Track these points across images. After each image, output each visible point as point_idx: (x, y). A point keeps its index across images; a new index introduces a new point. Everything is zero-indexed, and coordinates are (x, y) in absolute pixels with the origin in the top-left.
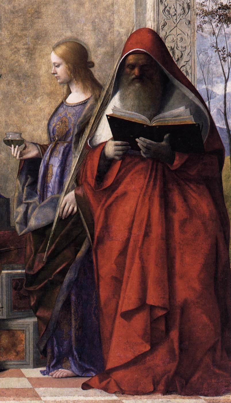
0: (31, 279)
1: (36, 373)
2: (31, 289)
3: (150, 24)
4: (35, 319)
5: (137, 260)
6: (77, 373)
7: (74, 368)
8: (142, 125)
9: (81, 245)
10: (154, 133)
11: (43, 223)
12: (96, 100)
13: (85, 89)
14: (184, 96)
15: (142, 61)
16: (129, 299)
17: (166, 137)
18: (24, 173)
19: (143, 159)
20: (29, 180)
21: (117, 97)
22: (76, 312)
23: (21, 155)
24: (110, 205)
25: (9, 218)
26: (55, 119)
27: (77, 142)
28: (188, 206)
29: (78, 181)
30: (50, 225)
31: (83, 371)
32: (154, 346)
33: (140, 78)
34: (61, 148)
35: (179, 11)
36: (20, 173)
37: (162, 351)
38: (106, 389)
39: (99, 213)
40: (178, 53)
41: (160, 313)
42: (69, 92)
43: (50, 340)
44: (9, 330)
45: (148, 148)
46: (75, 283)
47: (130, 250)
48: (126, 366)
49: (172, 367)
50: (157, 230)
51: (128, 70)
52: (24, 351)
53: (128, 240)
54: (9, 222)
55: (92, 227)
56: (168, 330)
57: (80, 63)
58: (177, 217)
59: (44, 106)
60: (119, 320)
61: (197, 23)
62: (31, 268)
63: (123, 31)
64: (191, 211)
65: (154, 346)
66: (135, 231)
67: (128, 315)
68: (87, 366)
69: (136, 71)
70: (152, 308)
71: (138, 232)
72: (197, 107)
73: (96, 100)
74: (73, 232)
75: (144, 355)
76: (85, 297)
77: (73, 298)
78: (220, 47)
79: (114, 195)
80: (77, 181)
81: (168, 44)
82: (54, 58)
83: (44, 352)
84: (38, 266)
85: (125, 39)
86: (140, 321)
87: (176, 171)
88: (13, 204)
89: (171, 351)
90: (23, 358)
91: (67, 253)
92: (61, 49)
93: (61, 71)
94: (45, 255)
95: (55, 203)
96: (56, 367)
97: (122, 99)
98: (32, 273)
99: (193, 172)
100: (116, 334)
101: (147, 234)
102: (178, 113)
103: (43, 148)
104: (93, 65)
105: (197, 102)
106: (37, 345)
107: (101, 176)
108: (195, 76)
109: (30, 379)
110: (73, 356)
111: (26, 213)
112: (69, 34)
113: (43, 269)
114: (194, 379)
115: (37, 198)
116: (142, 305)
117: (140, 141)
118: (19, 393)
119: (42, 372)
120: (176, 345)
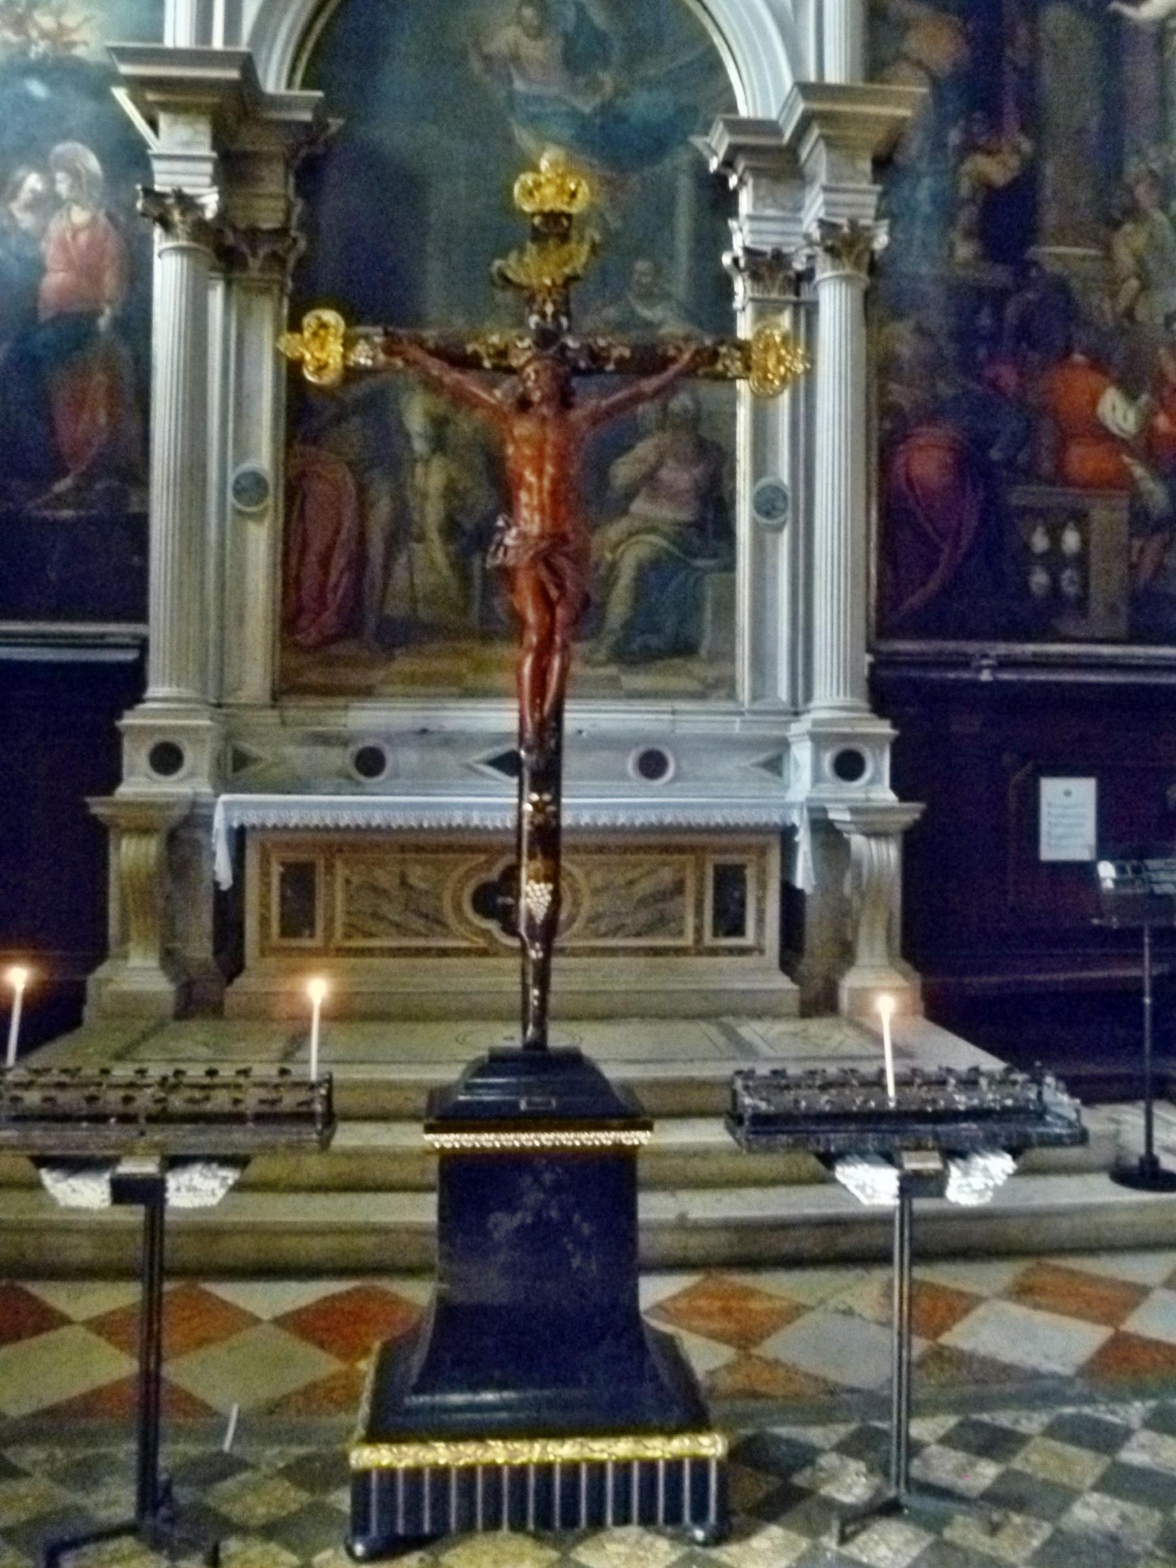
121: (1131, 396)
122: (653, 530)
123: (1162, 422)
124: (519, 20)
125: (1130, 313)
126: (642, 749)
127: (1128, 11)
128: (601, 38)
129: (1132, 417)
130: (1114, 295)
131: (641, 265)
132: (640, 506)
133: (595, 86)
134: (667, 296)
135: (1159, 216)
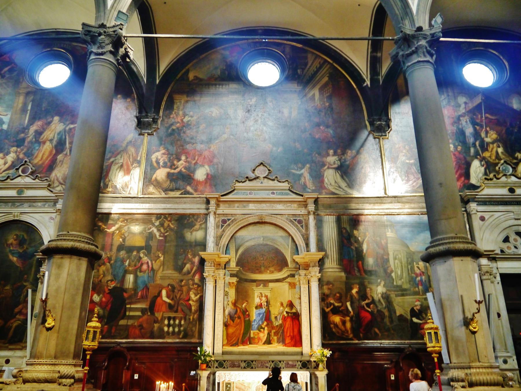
0: (276, 332)
1: (277, 344)
16: (288, 334)
29: (282, 319)
46: (282, 333)
57: (282, 304)
59: (277, 310)
74: (281, 325)
86: (290, 337)
93: (280, 305)
102: (294, 311)
116: (290, 335)
121: (99, 295)
122: (19, 320)
123: (104, 299)
124: (13, 238)
125: (101, 281)
126: (6, 359)
127: (108, 230)
128: (25, 240)
129: (98, 299)
130: (98, 278)
131: (26, 276)
132: (18, 316)
133: (23, 247)
134: (28, 281)
135: (108, 264)
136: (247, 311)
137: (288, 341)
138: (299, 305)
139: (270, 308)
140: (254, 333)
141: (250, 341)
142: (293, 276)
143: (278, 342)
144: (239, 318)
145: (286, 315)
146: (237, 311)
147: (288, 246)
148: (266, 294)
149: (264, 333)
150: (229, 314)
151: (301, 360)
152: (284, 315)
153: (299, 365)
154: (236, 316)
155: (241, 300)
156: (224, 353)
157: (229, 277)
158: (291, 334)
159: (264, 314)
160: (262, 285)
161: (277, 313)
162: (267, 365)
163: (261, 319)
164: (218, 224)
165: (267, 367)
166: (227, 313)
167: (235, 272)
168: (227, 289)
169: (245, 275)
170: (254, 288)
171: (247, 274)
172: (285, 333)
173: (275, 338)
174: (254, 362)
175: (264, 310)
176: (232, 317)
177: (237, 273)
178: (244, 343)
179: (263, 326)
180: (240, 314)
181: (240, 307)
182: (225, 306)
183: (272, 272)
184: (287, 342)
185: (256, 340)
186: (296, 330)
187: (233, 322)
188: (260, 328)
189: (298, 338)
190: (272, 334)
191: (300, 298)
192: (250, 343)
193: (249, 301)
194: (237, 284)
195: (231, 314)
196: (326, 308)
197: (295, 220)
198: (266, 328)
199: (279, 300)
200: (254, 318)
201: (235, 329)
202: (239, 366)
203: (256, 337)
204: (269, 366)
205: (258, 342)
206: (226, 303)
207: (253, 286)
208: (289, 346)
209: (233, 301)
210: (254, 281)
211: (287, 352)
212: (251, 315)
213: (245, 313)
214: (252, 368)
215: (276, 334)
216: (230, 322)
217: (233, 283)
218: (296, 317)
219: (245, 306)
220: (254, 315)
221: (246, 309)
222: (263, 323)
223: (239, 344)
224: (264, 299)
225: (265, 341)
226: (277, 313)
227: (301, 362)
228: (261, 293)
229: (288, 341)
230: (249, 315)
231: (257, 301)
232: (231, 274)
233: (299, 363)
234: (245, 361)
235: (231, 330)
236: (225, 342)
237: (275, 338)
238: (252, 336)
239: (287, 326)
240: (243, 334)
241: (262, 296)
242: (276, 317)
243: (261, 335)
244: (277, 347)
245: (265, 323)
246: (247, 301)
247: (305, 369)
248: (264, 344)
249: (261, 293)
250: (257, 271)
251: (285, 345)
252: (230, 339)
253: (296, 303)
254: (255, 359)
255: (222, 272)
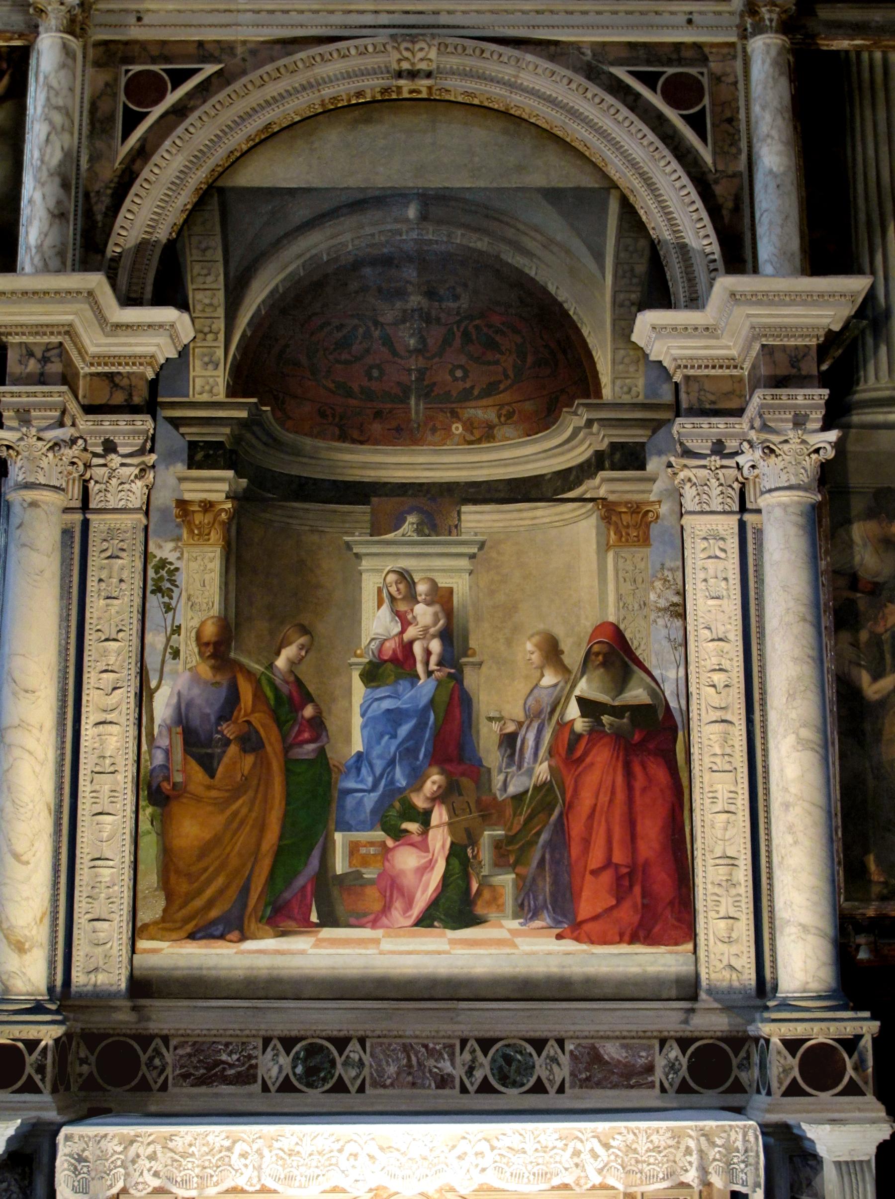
0: (511, 839)
1: (515, 924)
2: (510, 848)
3: (612, 619)
4: (514, 876)
5: (603, 823)
6: (552, 924)
7: (548, 920)
8: (606, 705)
9: (553, 810)
10: (617, 711)
11: (521, 789)
12: (566, 683)
13: (556, 672)
14: (642, 679)
15: (605, 648)
16: (596, 858)
17: (627, 714)
18: (504, 745)
19: (608, 734)
20: (509, 752)
21: (584, 680)
22: (550, 869)
23: (501, 730)
24: (579, 775)
25: (490, 785)
26: (531, 698)
27: (550, 719)
28: (647, 774)
29: (551, 753)
30: (527, 791)
31: (558, 923)
32: (620, 900)
33: (604, 664)
34: (535, 725)
35: (636, 607)
36: (500, 745)
37: (627, 905)
38: (578, 939)
39: (569, 782)
40: (636, 643)
41: (625, 870)
42: (542, 675)
43: (527, 894)
44: (491, 886)
45: (611, 725)
46: (550, 844)
47: (597, 814)
48: (595, 918)
49: (636, 919)
50: (620, 796)
51: (593, 657)
52: (503, 904)
53: (596, 805)
54: (490, 790)
55: (563, 793)
56: (631, 887)
57: (552, 651)
58: (639, 783)
59: (521, 688)
60: (588, 877)
61: (652, 617)
62: (510, 829)
63: (588, 624)
64: (649, 779)
65: (620, 900)
66: (601, 796)
67: (594, 873)
68: (560, 918)
69: (600, 658)
70: (617, 866)
71: (604, 798)
72: (654, 690)
73: (566, 683)
75: (612, 908)
76: (558, 856)
77: (547, 856)
78: (672, 638)
79: (583, 765)
80: (550, 753)
81: (628, 635)
82: (529, 646)
83: (522, 906)
84: (516, 828)
85: (590, 630)
86: (607, 877)
87: (635, 745)
88: (494, 773)
89: (635, 906)
90: (503, 911)
91: (542, 815)
92: (536, 639)
93: (536, 657)
94: (522, 818)
95: (530, 772)
96: (532, 919)
97: (589, 681)
98: (511, 834)
99: (651, 746)
100: (585, 888)
101: (611, 801)
102: (636, 694)
103: (520, 724)
104: (562, 652)
105: (653, 685)
106: (516, 899)
107: (571, 748)
108: (651, 663)
109: (509, 930)
110: (547, 909)
111: (505, 780)
112: (541, 626)
113: (520, 831)
114: (657, 929)
115: (514, 768)
116: (608, 863)
117: (605, 719)
118: (500, 943)
119: (521, 924)
120: (639, 900)
136: (308, 698)
137: (593, 897)
138: (672, 656)
139: (470, 679)
140: (353, 849)
141: (332, 904)
142: (630, 458)
143: (526, 909)
144: (250, 742)
145: (580, 725)
146: (233, 698)
147: (599, 257)
148: (443, 582)
149: (423, 846)
150: (182, 719)
151: (687, 1030)
152: (564, 726)
153: (672, 1067)
154: (229, 730)
155: (262, 625)
156: (141, 987)
157: (180, 468)
158: (618, 857)
159: (425, 711)
160: (412, 519)
161: (515, 710)
162: (446, 1066)
163: (408, 751)
164: (104, 107)
165: (443, 1082)
166: (163, 706)
167: (222, 434)
168: (164, 550)
169: (297, 452)
170: (359, 540)
171: (308, 442)
172: (575, 850)
173: (506, 880)
174: (354, 1050)
175: (426, 688)
176: (197, 740)
177: (237, 439)
178: (282, 917)
179: (420, 801)
180: (256, 719)
181: (257, 668)
182: (152, 661)
183: (485, 434)
184: (585, 909)
185: (372, 899)
186: (651, 830)
187: (211, 772)
188: (398, 817)
189: (662, 880)
190: (485, 854)
191: (679, 611)
192: (329, 920)
193: (322, 628)
194: (237, 515)
195: (196, 721)
196: (865, 678)
197: (649, 80)
198: (439, 815)
199: (535, 621)
200: (358, 745)
201: (219, 821)
202: (247, 1077)
203: (370, 874)
204: (458, 1072)
205: (386, 909)
206: (156, 640)
207: (352, 526)
208: (604, 941)
209: (210, 631)
210: (359, 492)
211: (589, 981)
212: (332, 724)
213: (295, 708)
214: (340, 1087)
215: (508, 853)
216: (188, 773)
217: (207, 506)
218: (652, 737)
219: (293, 663)
220: (357, 721)
221: (299, 683)
222: (417, 779)
223: (253, 926)
224: (424, 613)
225: (434, 904)
226: (520, 716)
227: (684, 1043)
228: (404, 576)
229: (593, 897)
230: (318, 725)
231: (377, 624)
232: (193, 446)
233: (674, 1052)
234: (288, 1043)
235: (191, 830)
236: (151, 912)
237: (506, 880)
238: (340, 866)
239: (586, 799)
240: (280, 852)
241: (412, 597)
242: (509, 741)
243: (407, 860)
244: (512, 946)
245: (434, 781)
246: (304, 630)
247: (710, 1096)
248: (425, 921)
249: (404, 576)
250: (377, 427)
251: (574, 928)
252: (183, 887)
253: (651, 643)
254: (359, 1029)
255: (129, 430)
